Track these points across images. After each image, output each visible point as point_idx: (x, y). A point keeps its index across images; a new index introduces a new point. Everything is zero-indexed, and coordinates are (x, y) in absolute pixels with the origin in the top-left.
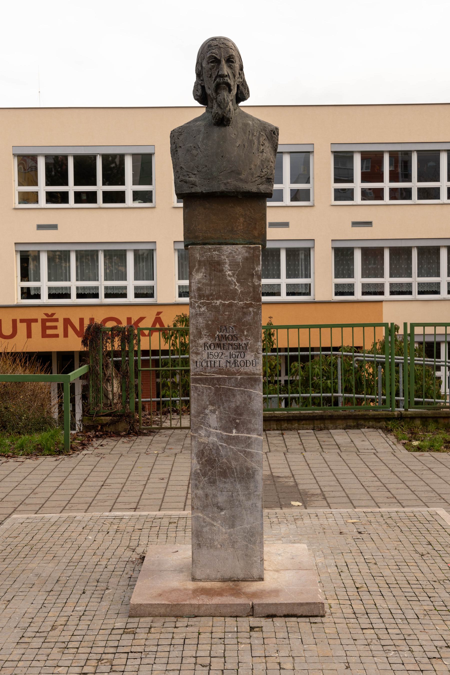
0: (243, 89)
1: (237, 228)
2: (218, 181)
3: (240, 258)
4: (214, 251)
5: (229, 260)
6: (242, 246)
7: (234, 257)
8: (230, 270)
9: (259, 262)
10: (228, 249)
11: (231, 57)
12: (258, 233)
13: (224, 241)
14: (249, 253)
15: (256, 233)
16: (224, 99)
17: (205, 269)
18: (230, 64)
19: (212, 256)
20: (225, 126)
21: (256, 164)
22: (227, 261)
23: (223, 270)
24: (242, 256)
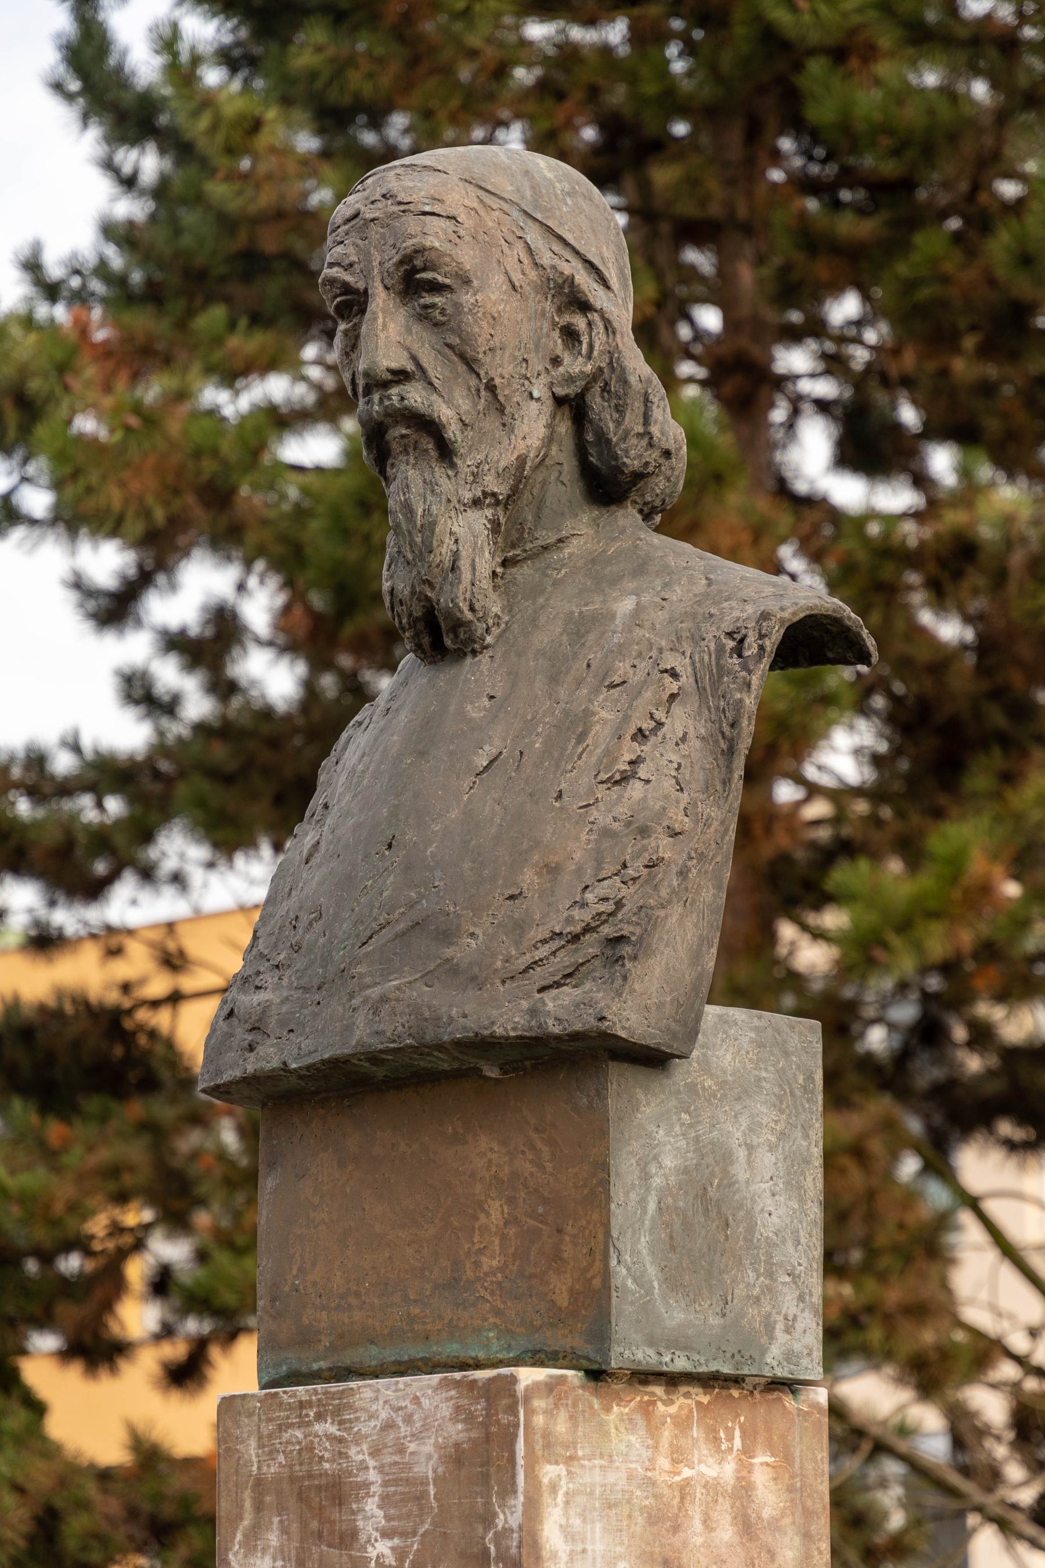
0: (606, 416)
1: (477, 1264)
2: (351, 996)
3: (429, 1457)
4: (320, 1417)
5: (381, 1469)
6: (436, 1378)
7: (401, 1451)
8: (386, 1534)
9: (514, 1476)
10: (376, 1398)
11: (418, 263)
12: (571, 1291)
13: (417, 1351)
14: (469, 1419)
15: (560, 1288)
16: (408, 509)
17: (284, 1530)
18: (428, 299)
19: (311, 1448)
20: (460, 655)
21: (554, 859)
22: (373, 1476)
23: (354, 1534)
24: (437, 1447)
